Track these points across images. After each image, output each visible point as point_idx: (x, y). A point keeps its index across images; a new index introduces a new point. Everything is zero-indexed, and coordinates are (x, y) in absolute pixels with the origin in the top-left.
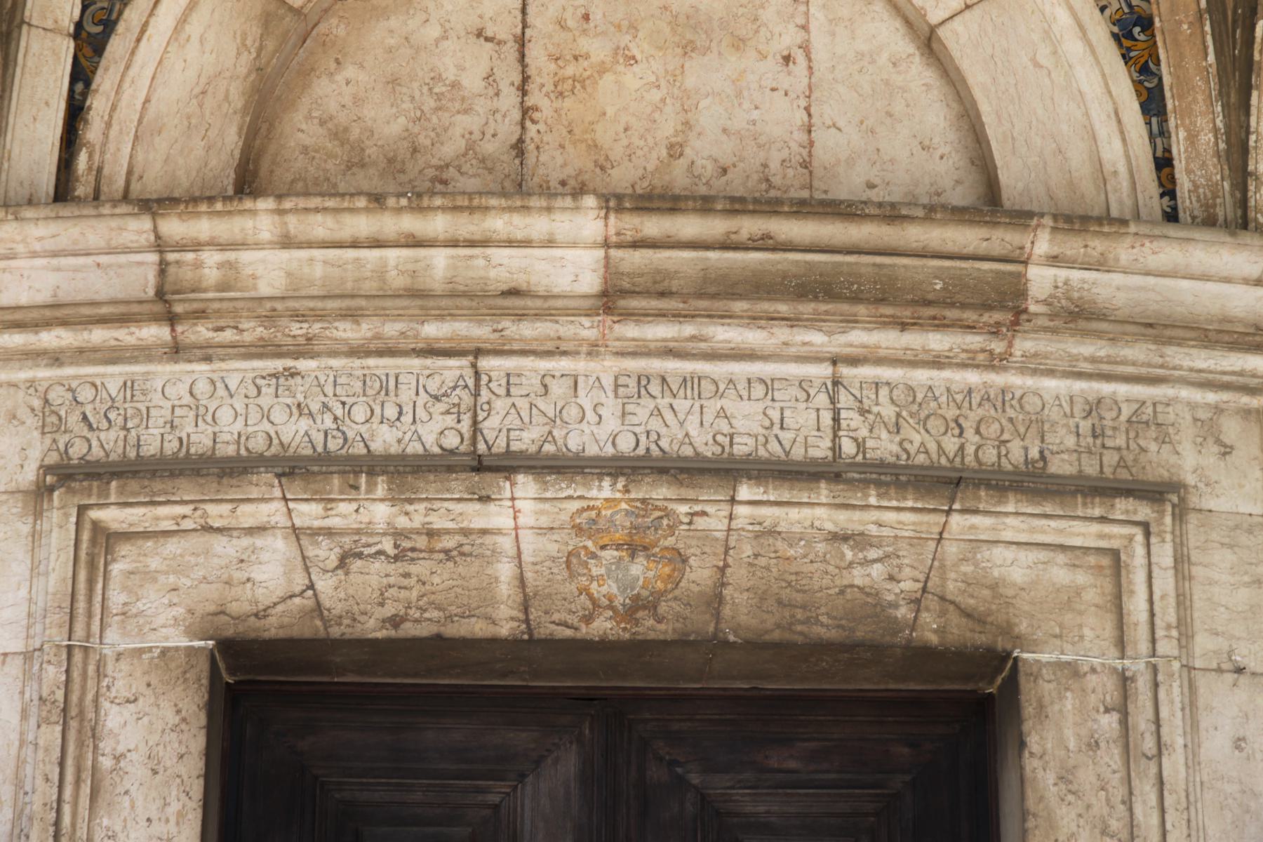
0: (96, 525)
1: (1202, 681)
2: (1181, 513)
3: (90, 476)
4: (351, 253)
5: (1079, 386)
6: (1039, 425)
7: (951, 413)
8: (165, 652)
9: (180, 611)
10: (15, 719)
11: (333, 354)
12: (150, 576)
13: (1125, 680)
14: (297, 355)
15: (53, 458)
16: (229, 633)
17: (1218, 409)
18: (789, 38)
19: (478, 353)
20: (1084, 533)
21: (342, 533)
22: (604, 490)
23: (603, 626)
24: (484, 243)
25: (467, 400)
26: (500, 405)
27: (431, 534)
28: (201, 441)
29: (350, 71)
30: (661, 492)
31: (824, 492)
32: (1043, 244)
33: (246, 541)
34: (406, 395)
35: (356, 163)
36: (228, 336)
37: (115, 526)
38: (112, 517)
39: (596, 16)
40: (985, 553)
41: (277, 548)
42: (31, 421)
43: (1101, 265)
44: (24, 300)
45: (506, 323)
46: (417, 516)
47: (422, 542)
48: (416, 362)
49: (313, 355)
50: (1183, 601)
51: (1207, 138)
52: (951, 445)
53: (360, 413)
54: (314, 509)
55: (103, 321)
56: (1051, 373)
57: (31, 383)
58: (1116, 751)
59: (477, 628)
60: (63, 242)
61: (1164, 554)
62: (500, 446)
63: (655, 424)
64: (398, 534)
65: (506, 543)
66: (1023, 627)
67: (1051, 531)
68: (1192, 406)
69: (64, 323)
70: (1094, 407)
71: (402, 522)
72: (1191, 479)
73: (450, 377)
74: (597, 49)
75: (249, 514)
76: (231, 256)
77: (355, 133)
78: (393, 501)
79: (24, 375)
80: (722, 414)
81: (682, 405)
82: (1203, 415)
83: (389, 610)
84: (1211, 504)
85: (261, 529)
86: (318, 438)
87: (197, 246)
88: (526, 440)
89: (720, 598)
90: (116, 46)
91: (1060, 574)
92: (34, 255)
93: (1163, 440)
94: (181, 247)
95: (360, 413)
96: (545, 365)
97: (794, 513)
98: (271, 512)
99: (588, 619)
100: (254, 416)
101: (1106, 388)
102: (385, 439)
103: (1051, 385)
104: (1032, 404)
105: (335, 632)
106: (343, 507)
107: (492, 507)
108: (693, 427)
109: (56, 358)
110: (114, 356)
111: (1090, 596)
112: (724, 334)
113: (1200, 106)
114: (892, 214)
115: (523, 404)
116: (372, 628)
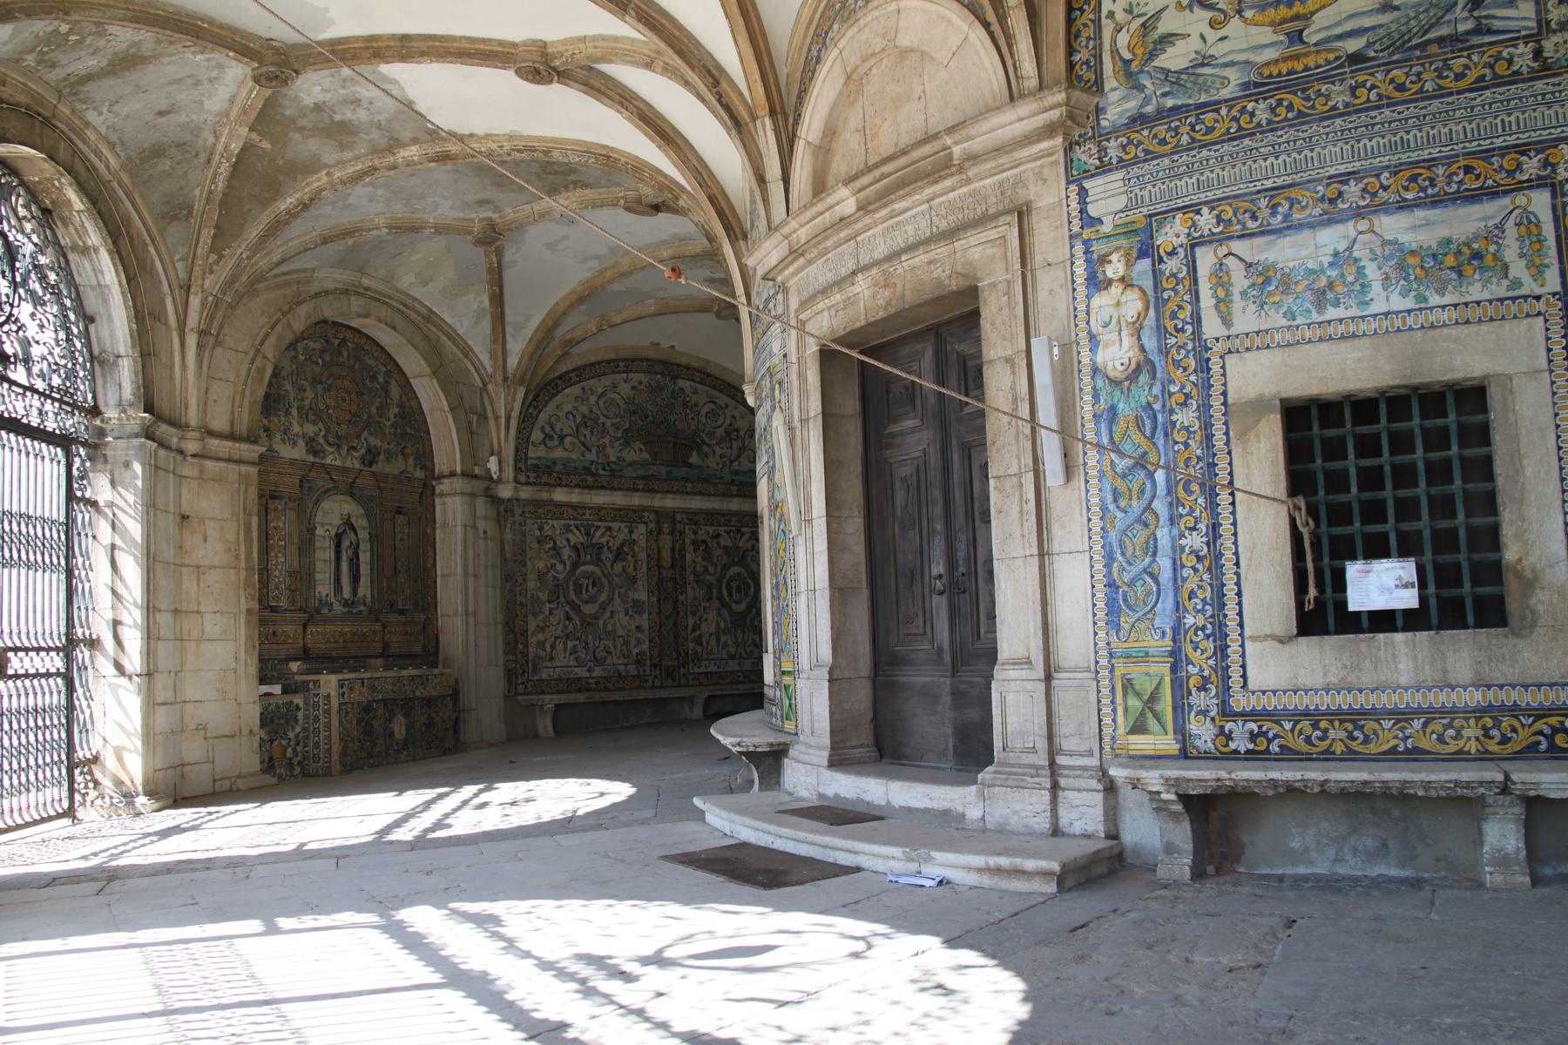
5: (996, 178)
17: (1042, 167)
23: (881, 314)
24: (832, 207)
30: (885, 266)
31: (921, 250)
32: (948, 141)
43: (969, 139)
52: (960, 216)
56: (986, 178)
59: (858, 325)
67: (983, 237)
70: (1001, 184)
74: (878, 121)
94: (790, 234)
96: (868, 234)
97: (916, 260)
101: (1004, 175)
103: (988, 182)
111: (999, 255)
112: (898, 206)
114: (904, 152)
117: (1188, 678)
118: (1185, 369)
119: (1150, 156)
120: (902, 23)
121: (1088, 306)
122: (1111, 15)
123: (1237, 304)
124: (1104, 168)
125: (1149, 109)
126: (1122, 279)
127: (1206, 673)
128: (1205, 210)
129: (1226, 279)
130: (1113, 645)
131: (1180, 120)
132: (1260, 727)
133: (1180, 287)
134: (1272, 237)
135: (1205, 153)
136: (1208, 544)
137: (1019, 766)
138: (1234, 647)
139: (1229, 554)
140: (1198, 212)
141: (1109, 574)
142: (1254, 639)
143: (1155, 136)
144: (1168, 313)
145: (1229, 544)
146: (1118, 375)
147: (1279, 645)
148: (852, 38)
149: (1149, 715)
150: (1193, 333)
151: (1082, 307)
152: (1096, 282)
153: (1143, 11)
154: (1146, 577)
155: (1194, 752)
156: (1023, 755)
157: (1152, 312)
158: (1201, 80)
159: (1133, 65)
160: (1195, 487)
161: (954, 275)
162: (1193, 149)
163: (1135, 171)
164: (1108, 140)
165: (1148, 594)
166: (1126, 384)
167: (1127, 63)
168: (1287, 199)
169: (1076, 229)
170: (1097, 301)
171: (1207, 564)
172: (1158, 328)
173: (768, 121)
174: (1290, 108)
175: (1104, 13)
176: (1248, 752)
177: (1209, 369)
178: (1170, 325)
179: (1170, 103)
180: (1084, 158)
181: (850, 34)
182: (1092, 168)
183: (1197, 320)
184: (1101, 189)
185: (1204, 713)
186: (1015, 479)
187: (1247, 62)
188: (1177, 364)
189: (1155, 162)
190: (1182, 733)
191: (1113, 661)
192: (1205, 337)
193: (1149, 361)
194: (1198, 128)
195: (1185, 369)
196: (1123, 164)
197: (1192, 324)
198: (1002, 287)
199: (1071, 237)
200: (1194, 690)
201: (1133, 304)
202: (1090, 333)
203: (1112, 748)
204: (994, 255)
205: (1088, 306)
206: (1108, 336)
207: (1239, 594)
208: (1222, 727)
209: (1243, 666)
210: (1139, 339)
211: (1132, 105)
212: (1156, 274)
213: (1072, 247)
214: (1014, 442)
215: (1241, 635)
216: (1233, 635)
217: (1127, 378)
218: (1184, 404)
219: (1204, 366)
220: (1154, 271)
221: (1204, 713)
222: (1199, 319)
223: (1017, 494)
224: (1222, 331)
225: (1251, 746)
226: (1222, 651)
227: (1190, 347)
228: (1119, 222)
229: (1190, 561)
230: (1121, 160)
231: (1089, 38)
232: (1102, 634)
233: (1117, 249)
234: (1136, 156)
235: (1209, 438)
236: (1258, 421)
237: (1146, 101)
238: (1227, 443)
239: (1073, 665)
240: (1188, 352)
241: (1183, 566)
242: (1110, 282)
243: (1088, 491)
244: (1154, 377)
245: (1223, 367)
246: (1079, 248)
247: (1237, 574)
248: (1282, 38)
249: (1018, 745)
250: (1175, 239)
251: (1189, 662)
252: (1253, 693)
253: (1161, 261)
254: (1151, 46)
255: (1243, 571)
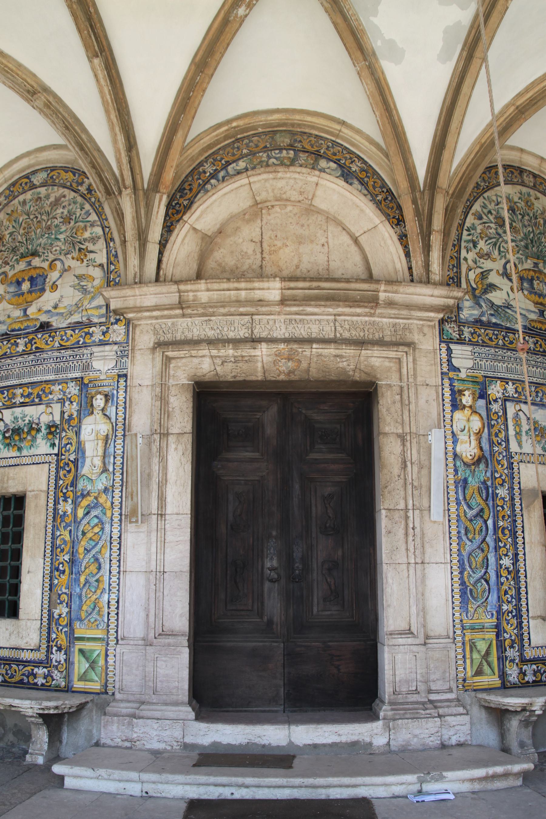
0: (167, 356)
1: (419, 387)
2: (414, 349)
3: (165, 345)
4: (223, 292)
5: (391, 320)
6: (382, 329)
7: (362, 327)
8: (183, 384)
9: (186, 375)
10: (150, 400)
11: (219, 316)
12: (179, 367)
13: (401, 388)
14: (211, 316)
15: (156, 341)
16: (197, 380)
17: (423, 325)
18: (323, 240)
19: (252, 315)
20: (392, 354)
21: (222, 357)
22: (282, 346)
23: (282, 377)
24: (253, 289)
25: (250, 326)
26: (258, 327)
27: (243, 357)
28: (189, 336)
29: (222, 250)
30: (295, 346)
31: (333, 346)
32: (383, 287)
33: (200, 359)
34: (236, 325)
35: (224, 271)
36: (195, 312)
37: (171, 356)
38: (170, 354)
39: (279, 236)
40: (370, 359)
41: (208, 360)
42: (152, 332)
43: (396, 292)
44: (149, 305)
45: (259, 308)
46: (239, 353)
47: (240, 358)
48: (238, 317)
49: (215, 316)
50: (415, 369)
51: (420, 262)
53: (226, 329)
54: (216, 351)
55: (167, 309)
56: (385, 317)
57: (151, 324)
58: (399, 404)
59: (253, 378)
60: (158, 291)
61: (410, 359)
62: (258, 336)
63: (294, 331)
64: (235, 357)
65: (260, 359)
66: (378, 376)
67: (385, 354)
68: (417, 325)
69: (158, 310)
70: (395, 325)
71: (236, 354)
72: (417, 342)
73: (246, 320)
74: (279, 243)
75: (201, 353)
76: (195, 293)
77: (223, 264)
78: (234, 349)
79: (149, 322)
80: (309, 328)
81: (300, 326)
82: (419, 327)
83: (233, 374)
84: (422, 347)
85: (203, 356)
86: (216, 335)
87: (187, 291)
88: (264, 335)
89: (309, 370)
90: (169, 246)
91: (387, 364)
92: (151, 294)
93: (410, 332)
94: (184, 292)
95: (226, 329)
96: (268, 317)
97: (326, 351)
98: (206, 352)
99: (279, 376)
100: (202, 330)
101: (397, 321)
102: (231, 335)
103: (385, 320)
104: (380, 324)
105: (221, 379)
106: (222, 351)
107: (256, 350)
108: (302, 331)
109: (157, 318)
110: (169, 317)
111: (394, 368)
112: (309, 309)
113: (418, 255)
114: (348, 281)
115: (263, 326)
116: (229, 378)
117: (505, 640)
118: (502, 466)
119: (484, 344)
120: (319, 192)
121: (452, 417)
122: (466, 259)
123: (524, 438)
124: (461, 341)
125: (484, 319)
126: (470, 407)
127: (513, 638)
128: (510, 383)
129: (519, 422)
130: (464, 622)
131: (498, 331)
132: (538, 667)
133: (499, 420)
134: (537, 408)
135: (509, 353)
136: (513, 564)
137: (407, 703)
138: (525, 623)
139: (522, 571)
140: (507, 383)
141: (462, 578)
142: (533, 618)
143: (487, 335)
144: (494, 433)
145: (522, 565)
146: (468, 461)
147: (542, 621)
148: (266, 180)
149: (485, 663)
150: (505, 447)
151: (448, 416)
152: (456, 406)
153: (482, 265)
154: (483, 581)
155: (508, 684)
156: (408, 696)
157: (486, 430)
158: (507, 315)
159: (477, 292)
160: (507, 532)
161: (357, 371)
162: (504, 349)
163: (477, 349)
164: (464, 326)
165: (484, 591)
166: (473, 467)
167: (474, 289)
168: (541, 390)
169: (445, 370)
170: (458, 415)
171: (513, 575)
172: (489, 439)
173: (165, 198)
174: (541, 346)
175: (462, 257)
176: (534, 682)
177: (513, 469)
178: (495, 439)
179: (494, 320)
180: (450, 331)
181: (265, 176)
182: (455, 339)
183: (507, 441)
184: (460, 352)
185: (513, 661)
186: (401, 512)
187: (525, 316)
188: (499, 462)
189: (488, 349)
190: (503, 675)
191: (465, 631)
192: (511, 451)
193: (483, 456)
194: (506, 339)
195: (502, 466)
196: (470, 343)
197: (505, 442)
198: (397, 389)
199: (442, 373)
200: (508, 648)
201: (476, 424)
202: (453, 432)
203: (463, 686)
204: (391, 368)
205: (452, 417)
206: (463, 437)
207: (527, 593)
208: (521, 668)
209: (529, 633)
210: (480, 443)
211: (476, 312)
212: (488, 410)
213: (442, 379)
214: (402, 489)
215: (528, 616)
216: (525, 616)
217: (473, 464)
218: (502, 485)
219: (511, 466)
220: (487, 408)
221: (513, 661)
222: (508, 440)
223: (403, 522)
224: (518, 450)
225: (534, 678)
226: (520, 625)
227: (504, 454)
228: (469, 374)
229: (504, 573)
230: (470, 340)
231: (453, 266)
232: (457, 615)
233: (468, 389)
234: (477, 341)
235: (513, 505)
236: (534, 501)
237: (482, 314)
238: (521, 510)
239: (437, 634)
240: (503, 456)
241: (501, 576)
242: (464, 407)
243: (450, 527)
244: (487, 467)
245: (519, 469)
246: (447, 382)
247: (526, 582)
248: (537, 311)
249: (404, 689)
250: (497, 394)
251: (505, 632)
252: (533, 648)
253: (490, 403)
254: (485, 287)
255: (528, 580)
